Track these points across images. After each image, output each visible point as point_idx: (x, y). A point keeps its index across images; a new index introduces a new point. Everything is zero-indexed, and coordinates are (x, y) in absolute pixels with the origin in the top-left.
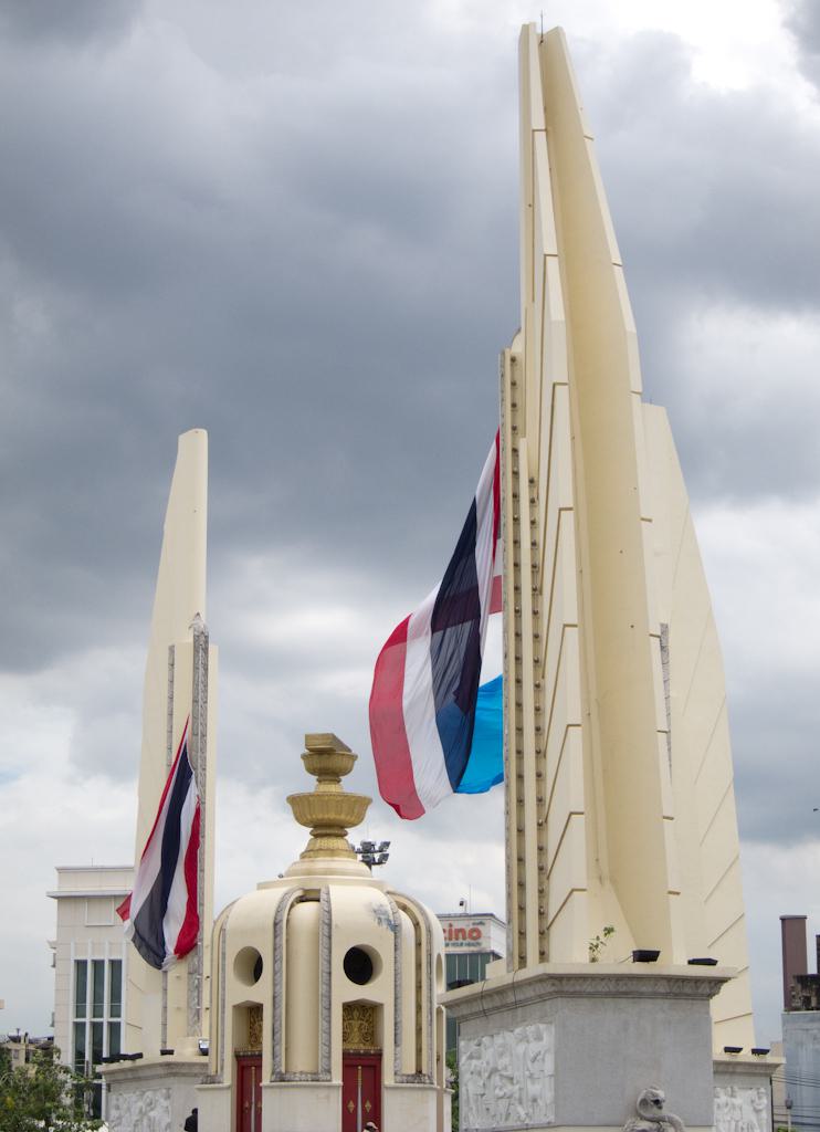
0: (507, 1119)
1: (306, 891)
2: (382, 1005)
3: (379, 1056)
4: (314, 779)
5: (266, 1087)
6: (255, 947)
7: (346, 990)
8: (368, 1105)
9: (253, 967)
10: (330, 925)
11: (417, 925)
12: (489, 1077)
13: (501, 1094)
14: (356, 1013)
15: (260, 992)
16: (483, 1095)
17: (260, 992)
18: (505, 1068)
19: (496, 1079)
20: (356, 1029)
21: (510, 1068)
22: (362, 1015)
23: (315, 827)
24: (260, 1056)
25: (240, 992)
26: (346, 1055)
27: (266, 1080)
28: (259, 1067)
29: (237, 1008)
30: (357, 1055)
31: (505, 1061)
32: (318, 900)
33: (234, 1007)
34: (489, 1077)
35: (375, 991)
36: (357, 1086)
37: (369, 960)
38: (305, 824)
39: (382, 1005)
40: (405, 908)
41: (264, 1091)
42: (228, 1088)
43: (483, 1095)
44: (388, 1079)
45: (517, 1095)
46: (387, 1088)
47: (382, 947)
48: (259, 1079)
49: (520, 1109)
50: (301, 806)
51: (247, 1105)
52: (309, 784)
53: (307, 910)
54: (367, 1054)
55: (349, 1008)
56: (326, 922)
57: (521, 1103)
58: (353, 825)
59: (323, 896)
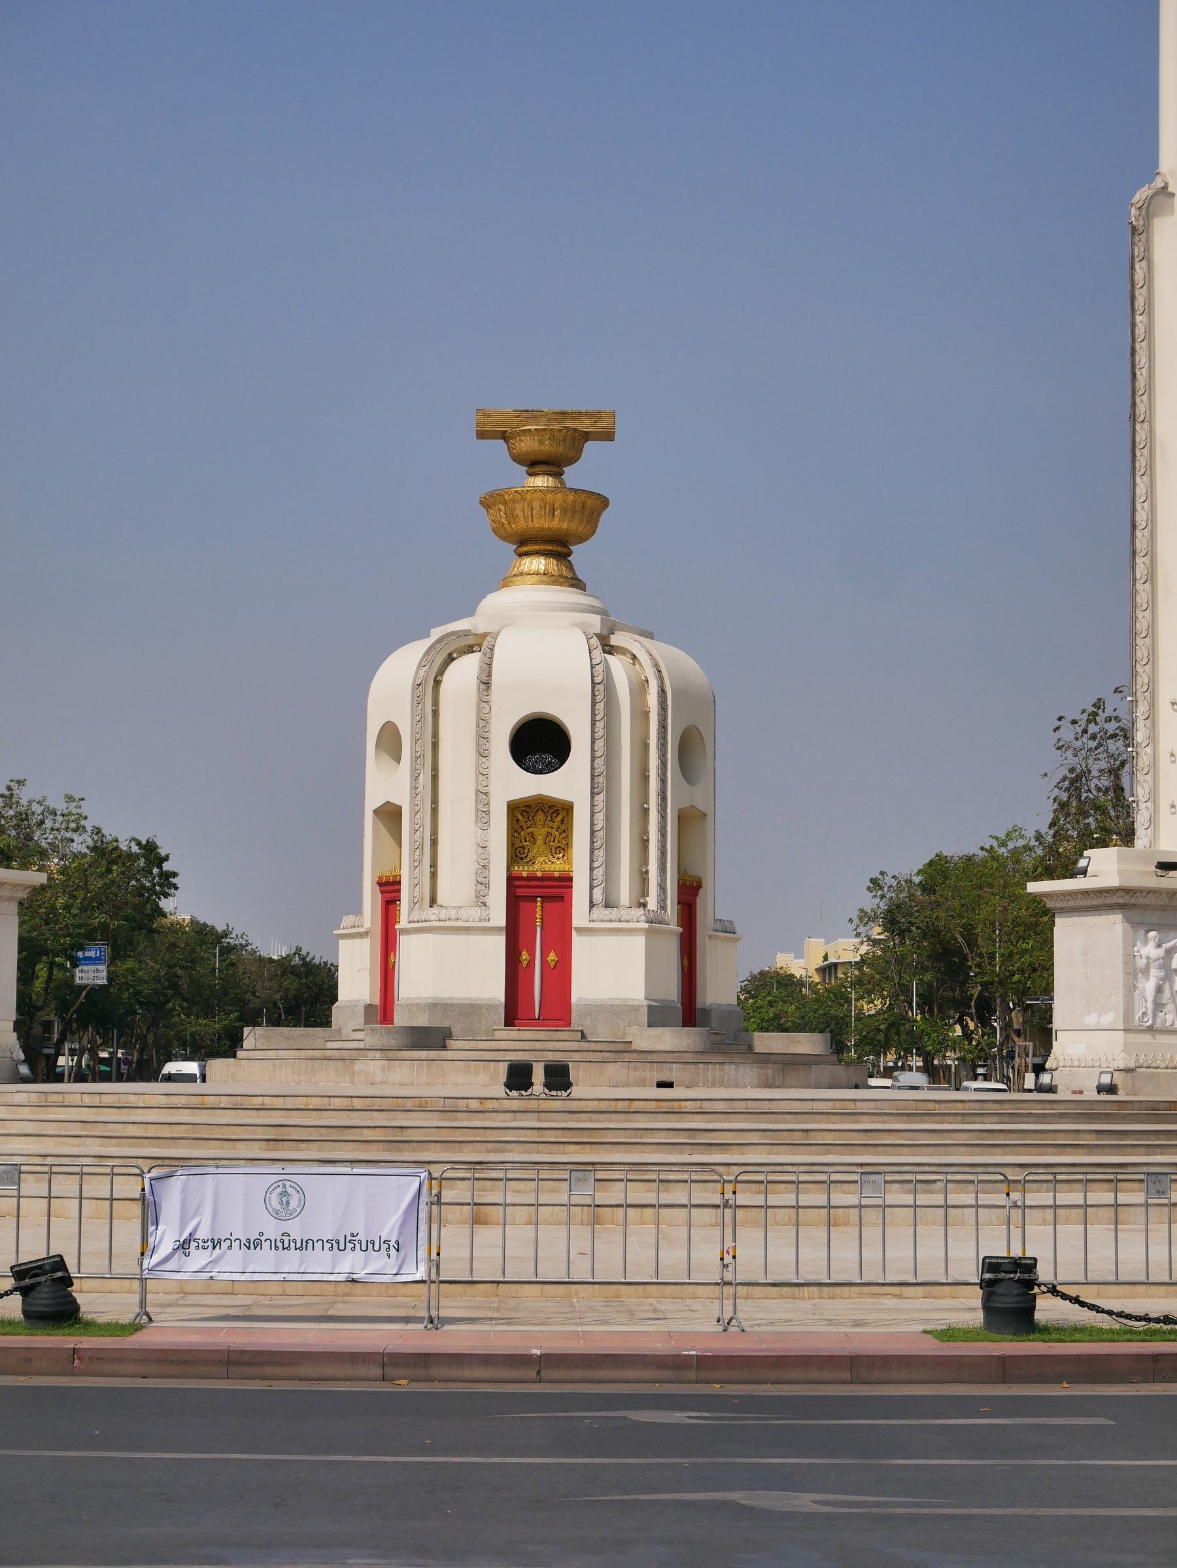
5: (407, 931)
8: (552, 957)
14: (540, 817)
38: (506, 538)
44: (580, 915)
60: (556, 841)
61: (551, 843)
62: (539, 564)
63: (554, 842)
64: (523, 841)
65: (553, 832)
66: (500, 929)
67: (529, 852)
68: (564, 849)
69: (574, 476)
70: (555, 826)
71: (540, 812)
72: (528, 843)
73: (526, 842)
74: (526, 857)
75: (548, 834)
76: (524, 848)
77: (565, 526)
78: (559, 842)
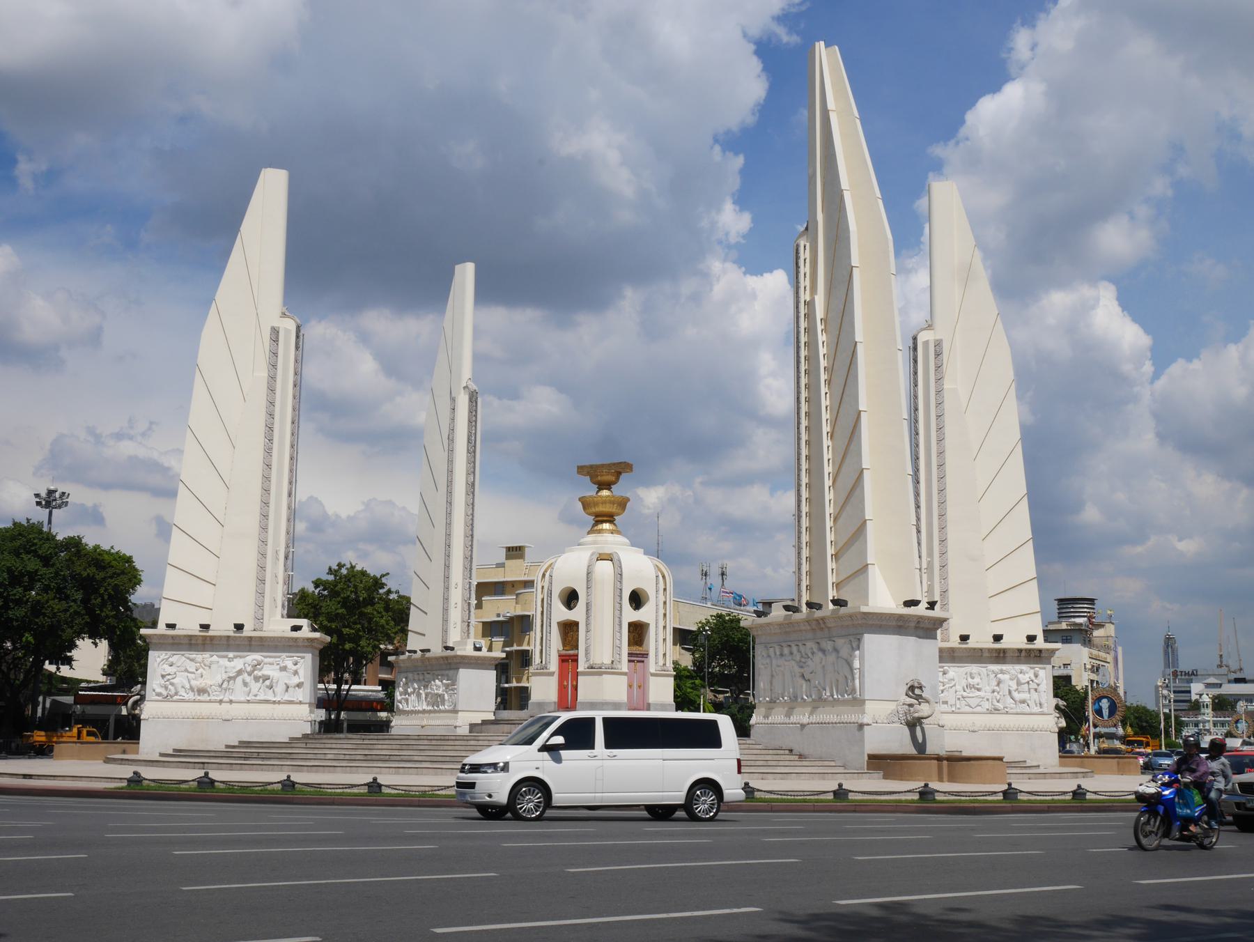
2: (649, 624)
6: (569, 586)
7: (630, 615)
9: (571, 598)
10: (621, 575)
11: (664, 577)
15: (577, 614)
17: (577, 614)
22: (638, 632)
23: (597, 516)
25: (561, 613)
26: (630, 655)
27: (580, 669)
33: (558, 623)
35: (644, 615)
39: (649, 624)
47: (650, 589)
50: (586, 504)
52: (590, 491)
53: (607, 565)
55: (630, 625)
56: (619, 576)
59: (615, 559)
62: (606, 526)
66: (625, 674)
69: (618, 490)
77: (610, 510)
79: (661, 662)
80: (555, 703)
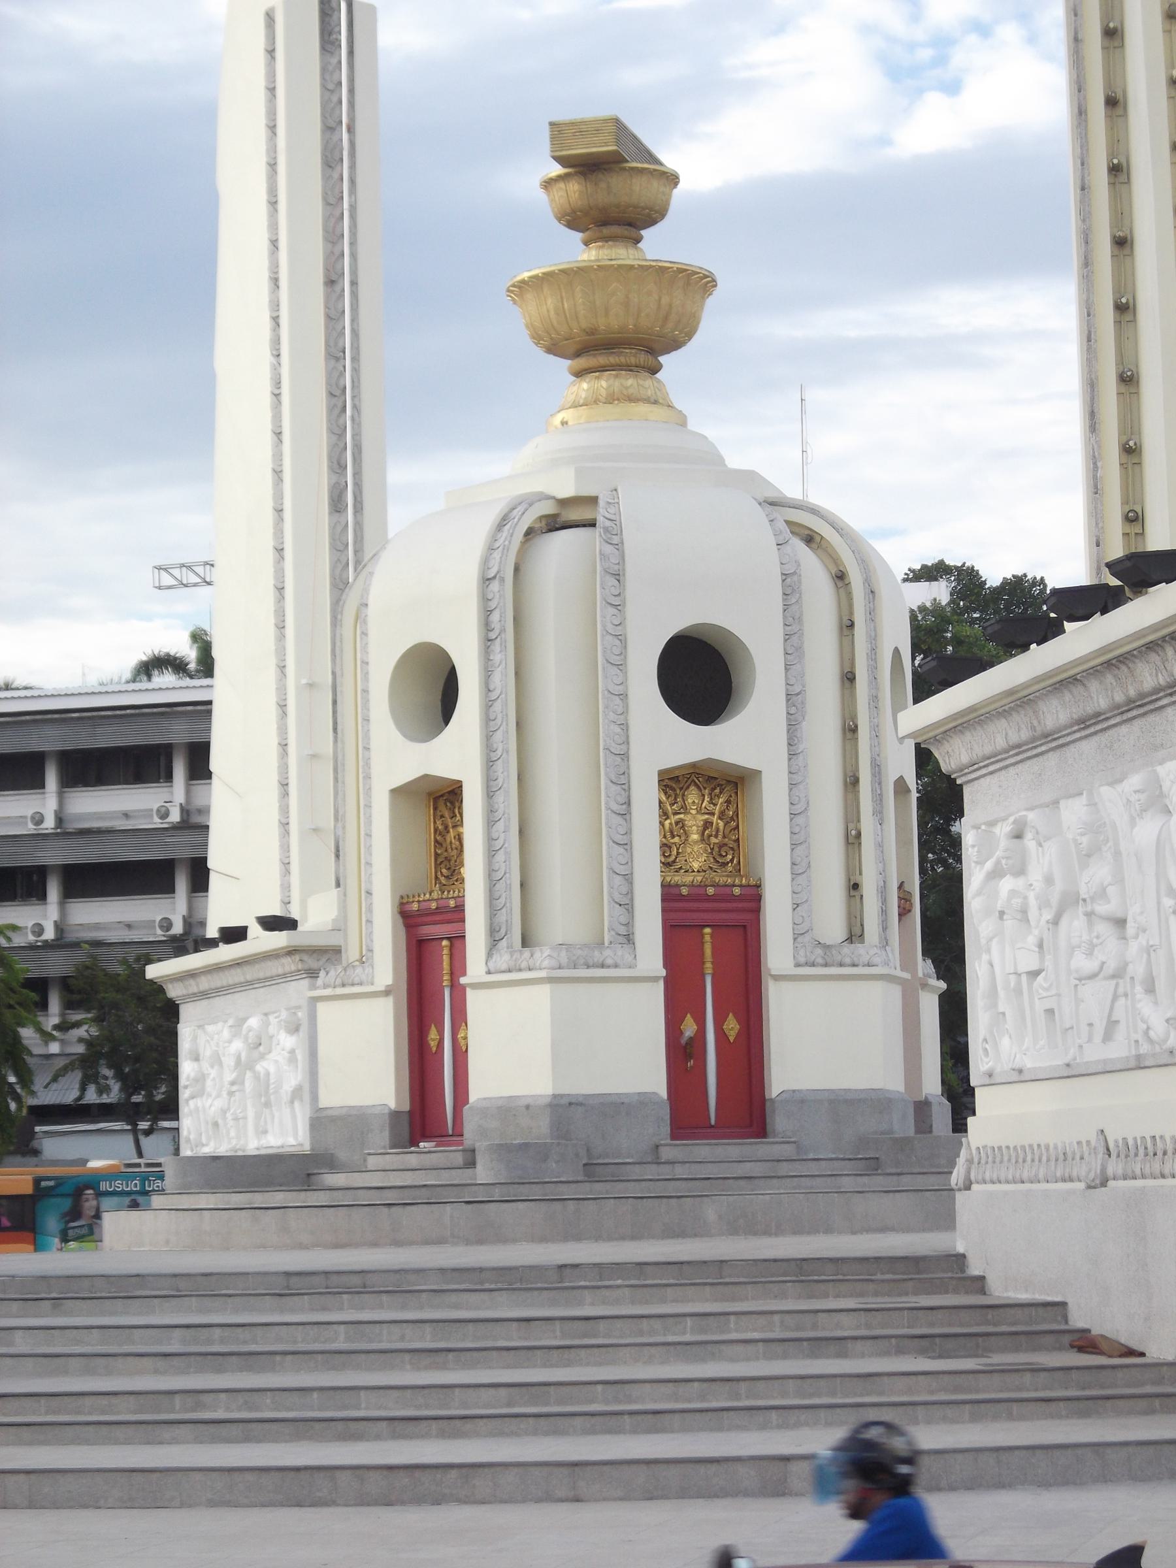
0: (1108, 1037)
1: (564, 503)
3: (753, 899)
4: (576, 237)
12: (1056, 922)
13: (1090, 966)
16: (1035, 974)
18: (1102, 894)
19: (1074, 925)
20: (695, 837)
21: (1111, 890)
24: (460, 909)
26: (670, 895)
28: (458, 940)
29: (398, 793)
30: (697, 896)
31: (1099, 873)
32: (592, 524)
34: (1056, 922)
36: (703, 976)
37: (720, 655)
40: (810, 539)
41: (470, 994)
42: (387, 992)
43: (1035, 974)
45: (1137, 969)
46: (777, 978)
48: (458, 966)
49: (1145, 1006)
51: (433, 1035)
54: (724, 897)
57: (1150, 989)
58: (675, 345)
59: (601, 514)
60: (720, 837)
61: (713, 840)
63: (716, 836)
64: (668, 834)
65: (715, 819)
66: (655, 979)
67: (678, 853)
68: (732, 849)
70: (717, 810)
71: (692, 787)
72: (676, 839)
73: (673, 837)
74: (674, 862)
75: (707, 824)
76: (670, 847)
78: (724, 837)
79: (833, 927)
80: (395, 1115)
